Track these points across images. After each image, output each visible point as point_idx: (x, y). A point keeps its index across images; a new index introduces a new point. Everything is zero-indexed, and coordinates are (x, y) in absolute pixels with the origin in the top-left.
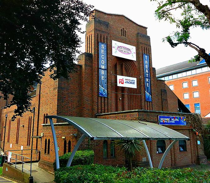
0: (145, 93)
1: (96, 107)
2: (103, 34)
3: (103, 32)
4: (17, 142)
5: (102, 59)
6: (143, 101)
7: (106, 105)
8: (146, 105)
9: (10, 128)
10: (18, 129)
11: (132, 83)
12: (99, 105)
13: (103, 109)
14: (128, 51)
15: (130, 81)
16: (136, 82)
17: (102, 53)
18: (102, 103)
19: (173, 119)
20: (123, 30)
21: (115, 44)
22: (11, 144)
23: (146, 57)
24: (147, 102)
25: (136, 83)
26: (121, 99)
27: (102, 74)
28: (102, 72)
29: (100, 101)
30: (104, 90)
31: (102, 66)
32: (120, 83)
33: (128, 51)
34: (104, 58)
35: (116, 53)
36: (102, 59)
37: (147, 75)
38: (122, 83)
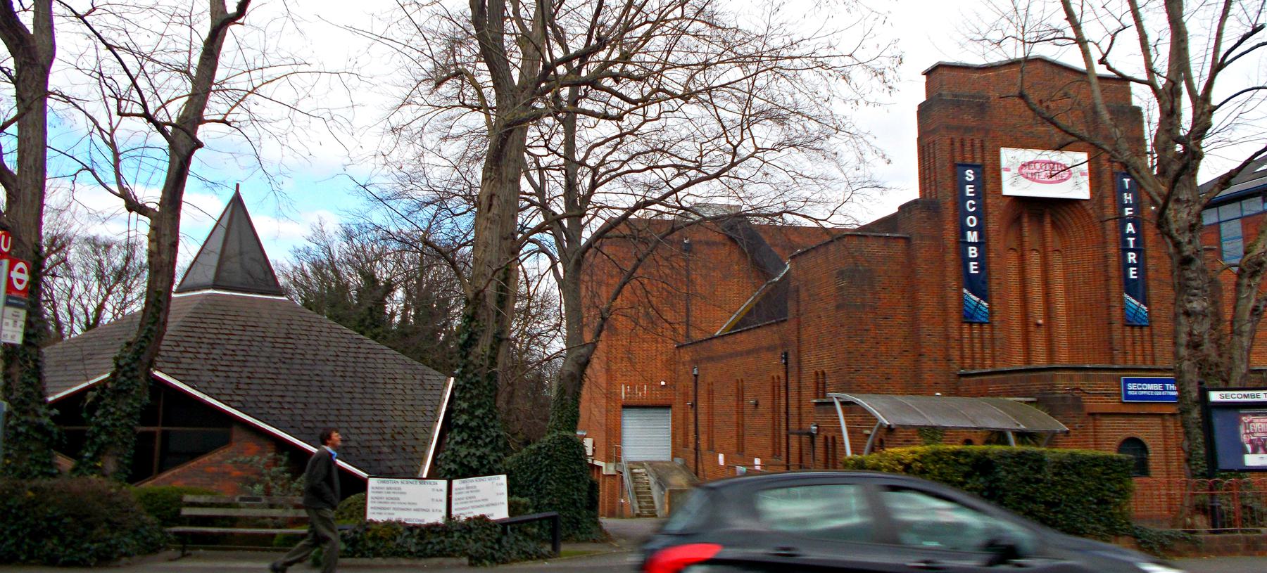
0: (1122, 300)
1: (955, 353)
2: (968, 137)
3: (968, 129)
4: (741, 449)
6: (1117, 325)
7: (988, 344)
8: (1129, 341)
9: (711, 409)
10: (740, 411)
12: (966, 345)
13: (978, 356)
17: (968, 195)
18: (976, 340)
21: (1010, 157)
22: (721, 457)
23: (1127, 180)
26: (1040, 321)
27: (971, 256)
28: (971, 252)
30: (978, 303)
31: (969, 233)
34: (974, 209)
35: (1013, 186)
36: (972, 214)
37: (1131, 239)
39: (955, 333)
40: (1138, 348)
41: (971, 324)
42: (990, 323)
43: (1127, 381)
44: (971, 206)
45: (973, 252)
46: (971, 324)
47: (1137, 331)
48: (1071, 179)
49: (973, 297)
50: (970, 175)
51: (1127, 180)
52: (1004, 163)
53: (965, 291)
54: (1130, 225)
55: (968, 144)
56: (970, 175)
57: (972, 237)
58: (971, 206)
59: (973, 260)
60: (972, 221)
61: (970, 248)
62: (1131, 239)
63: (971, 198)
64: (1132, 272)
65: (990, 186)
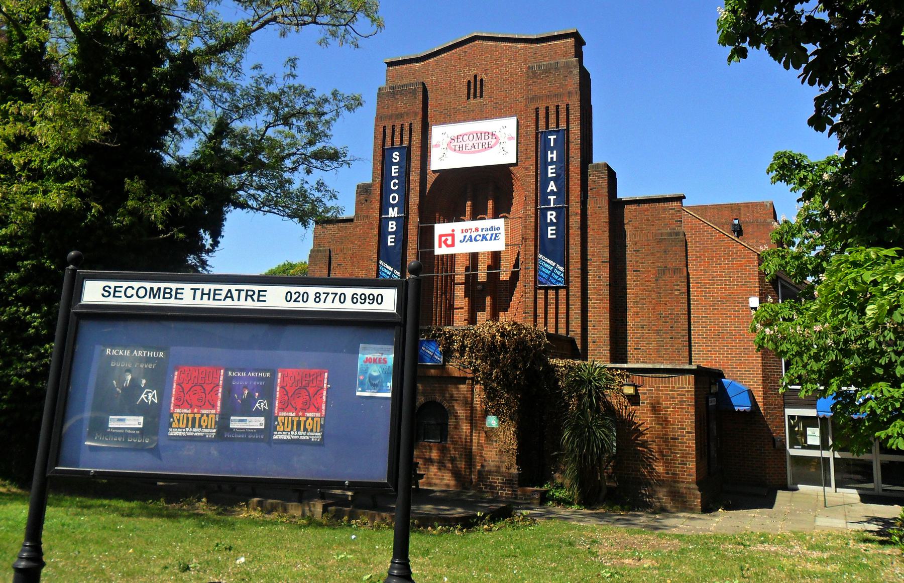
5: (394, 191)
11: (488, 237)
14: (487, 141)
15: (480, 233)
16: (502, 231)
17: (393, 174)
20: (472, 81)
21: (439, 134)
24: (546, 289)
25: (502, 237)
27: (390, 230)
28: (390, 226)
31: (391, 209)
32: (443, 245)
33: (487, 141)
34: (397, 187)
37: (552, 198)
38: (448, 246)
44: (395, 184)
45: (392, 226)
48: (498, 145)
49: (388, 267)
50: (396, 156)
51: (552, 138)
53: (381, 262)
54: (552, 183)
56: (396, 156)
58: (395, 184)
59: (391, 233)
60: (394, 198)
61: (390, 223)
62: (552, 198)
64: (551, 233)
65: (415, 163)
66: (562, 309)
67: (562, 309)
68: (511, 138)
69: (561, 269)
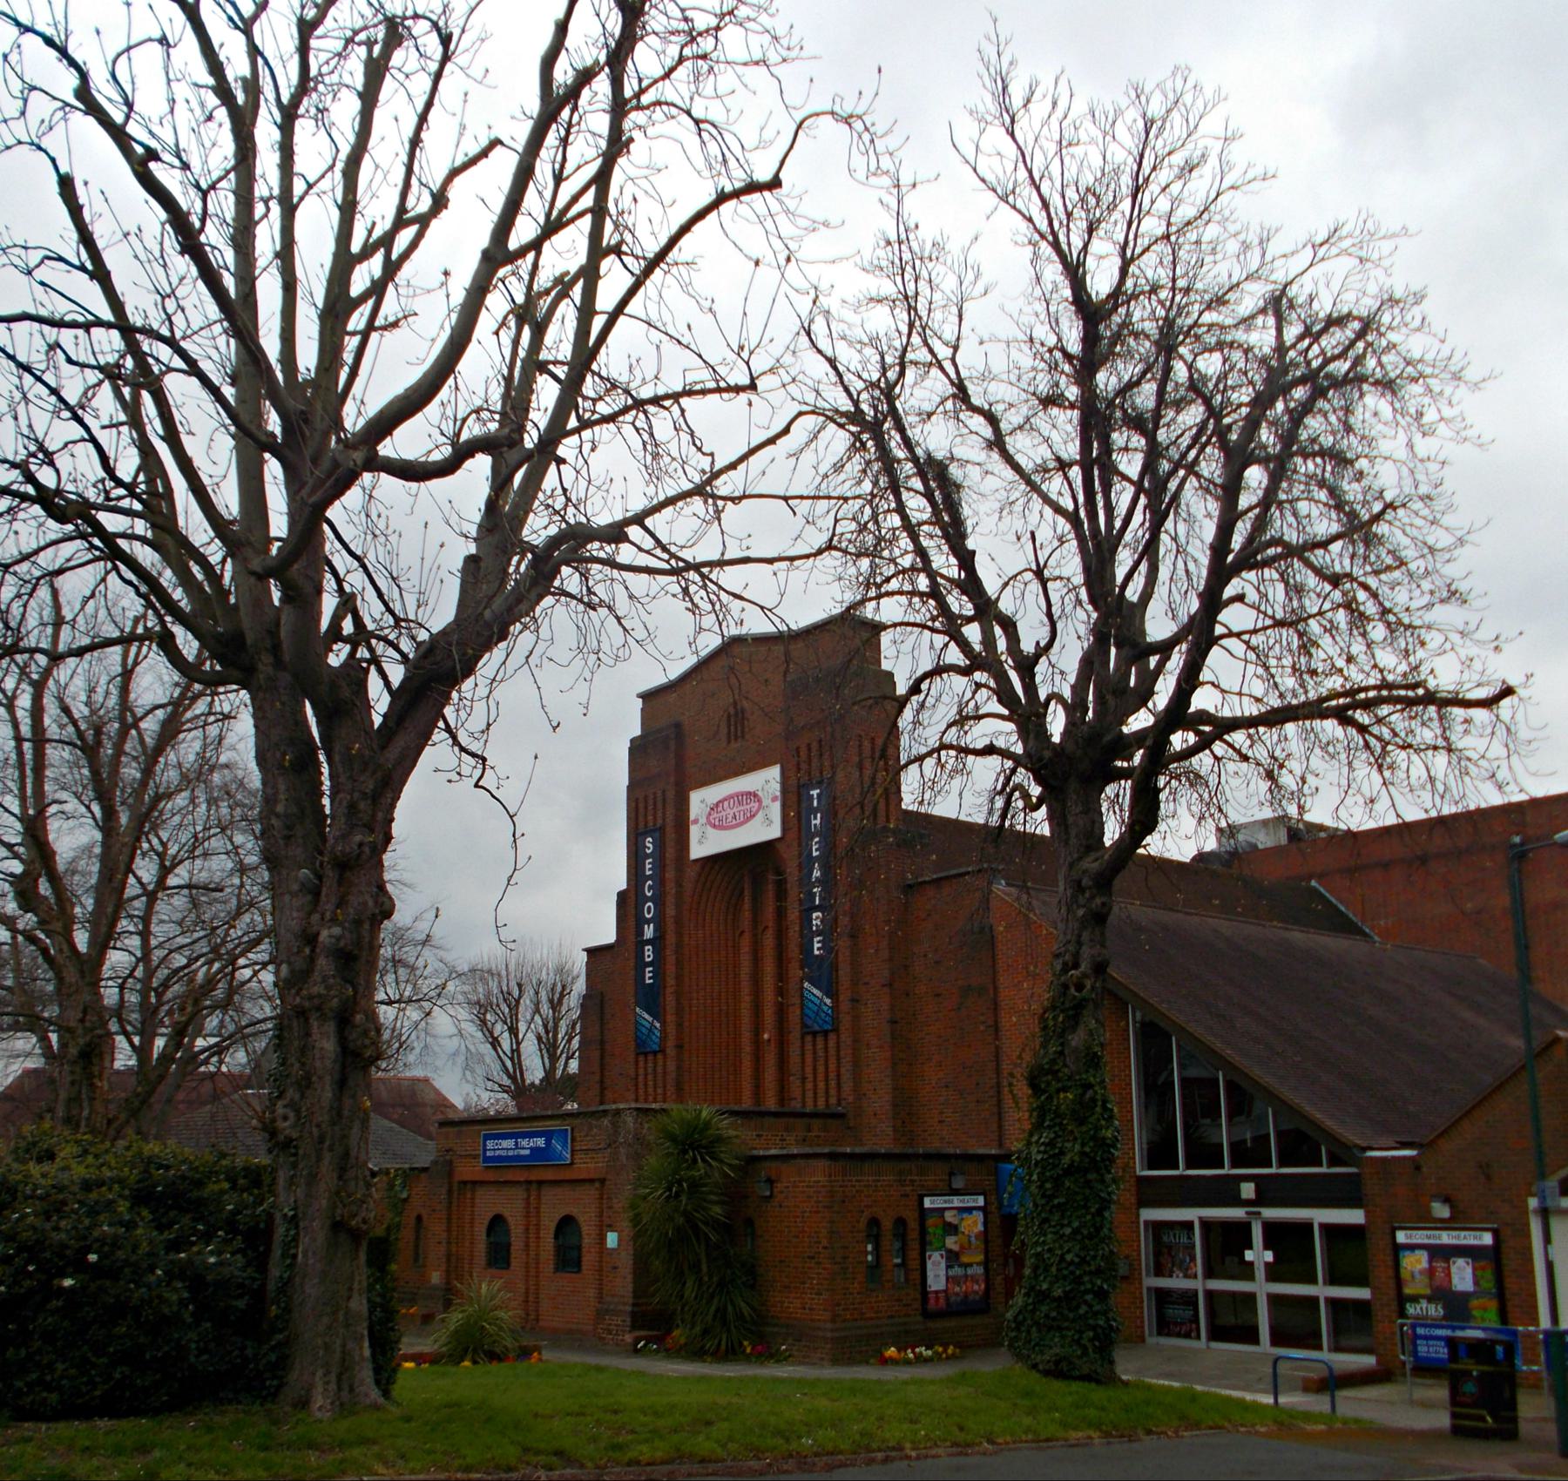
12: (641, 1085)
18: (650, 1077)
19: (524, 1142)
21: (700, 800)
24: (814, 1034)
29: (641, 1071)
35: (705, 843)
39: (632, 1072)
40: (821, 1069)
41: (646, 1054)
42: (663, 1051)
43: (487, 1137)
44: (650, 888)
45: (649, 952)
46: (646, 1054)
47: (820, 1040)
49: (646, 1016)
51: (815, 793)
52: (692, 817)
55: (651, 802)
57: (649, 932)
63: (649, 877)
65: (670, 853)
66: (832, 1067)
67: (832, 1067)
68: (774, 799)
69: (828, 1001)
